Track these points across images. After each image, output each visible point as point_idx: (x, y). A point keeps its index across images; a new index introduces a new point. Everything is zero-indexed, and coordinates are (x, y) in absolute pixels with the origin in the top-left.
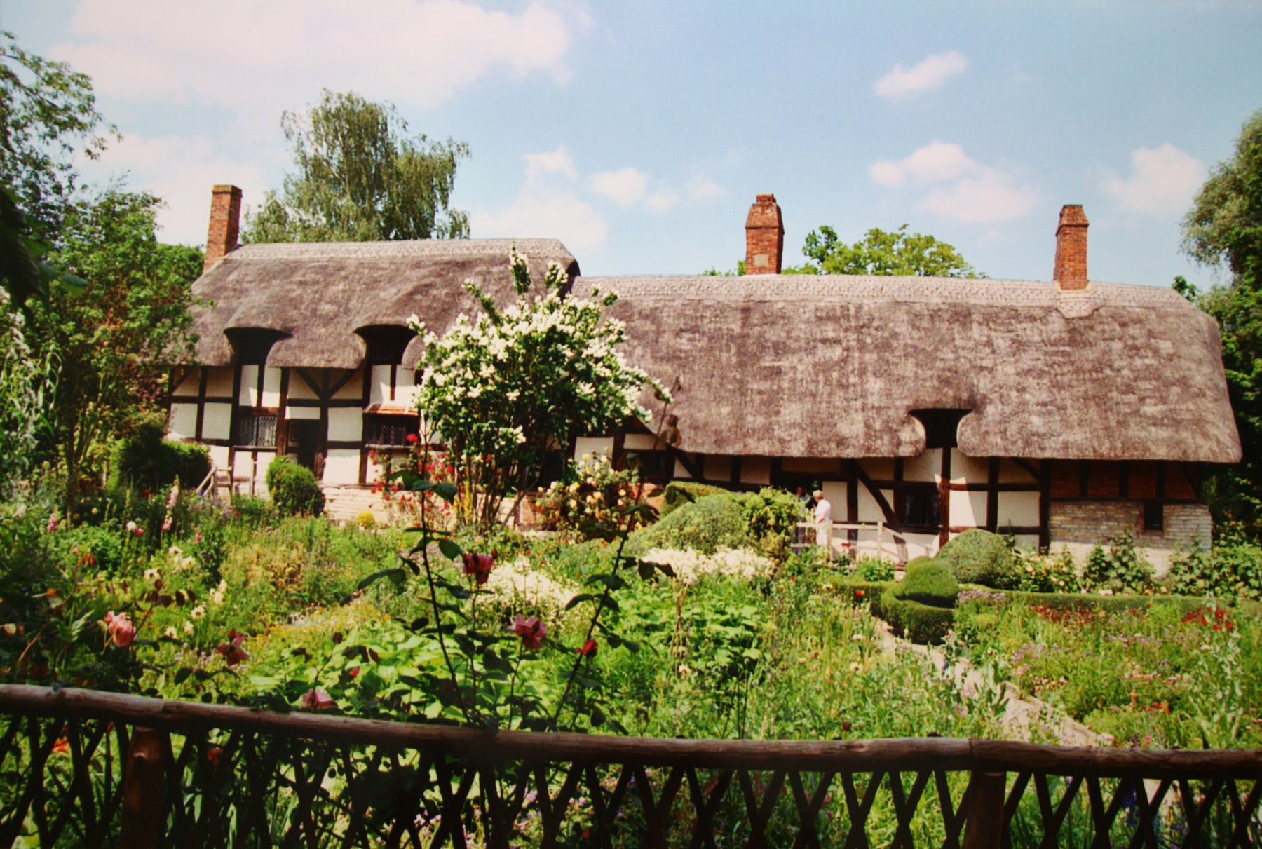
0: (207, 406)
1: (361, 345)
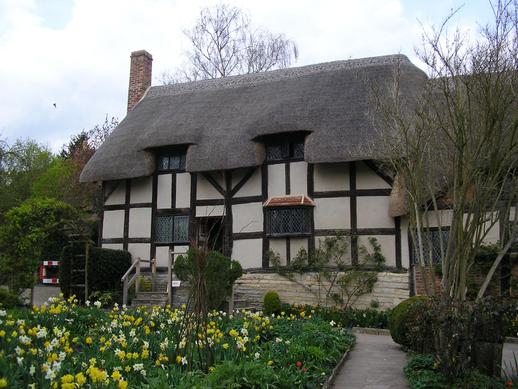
0: (132, 211)
1: (256, 147)
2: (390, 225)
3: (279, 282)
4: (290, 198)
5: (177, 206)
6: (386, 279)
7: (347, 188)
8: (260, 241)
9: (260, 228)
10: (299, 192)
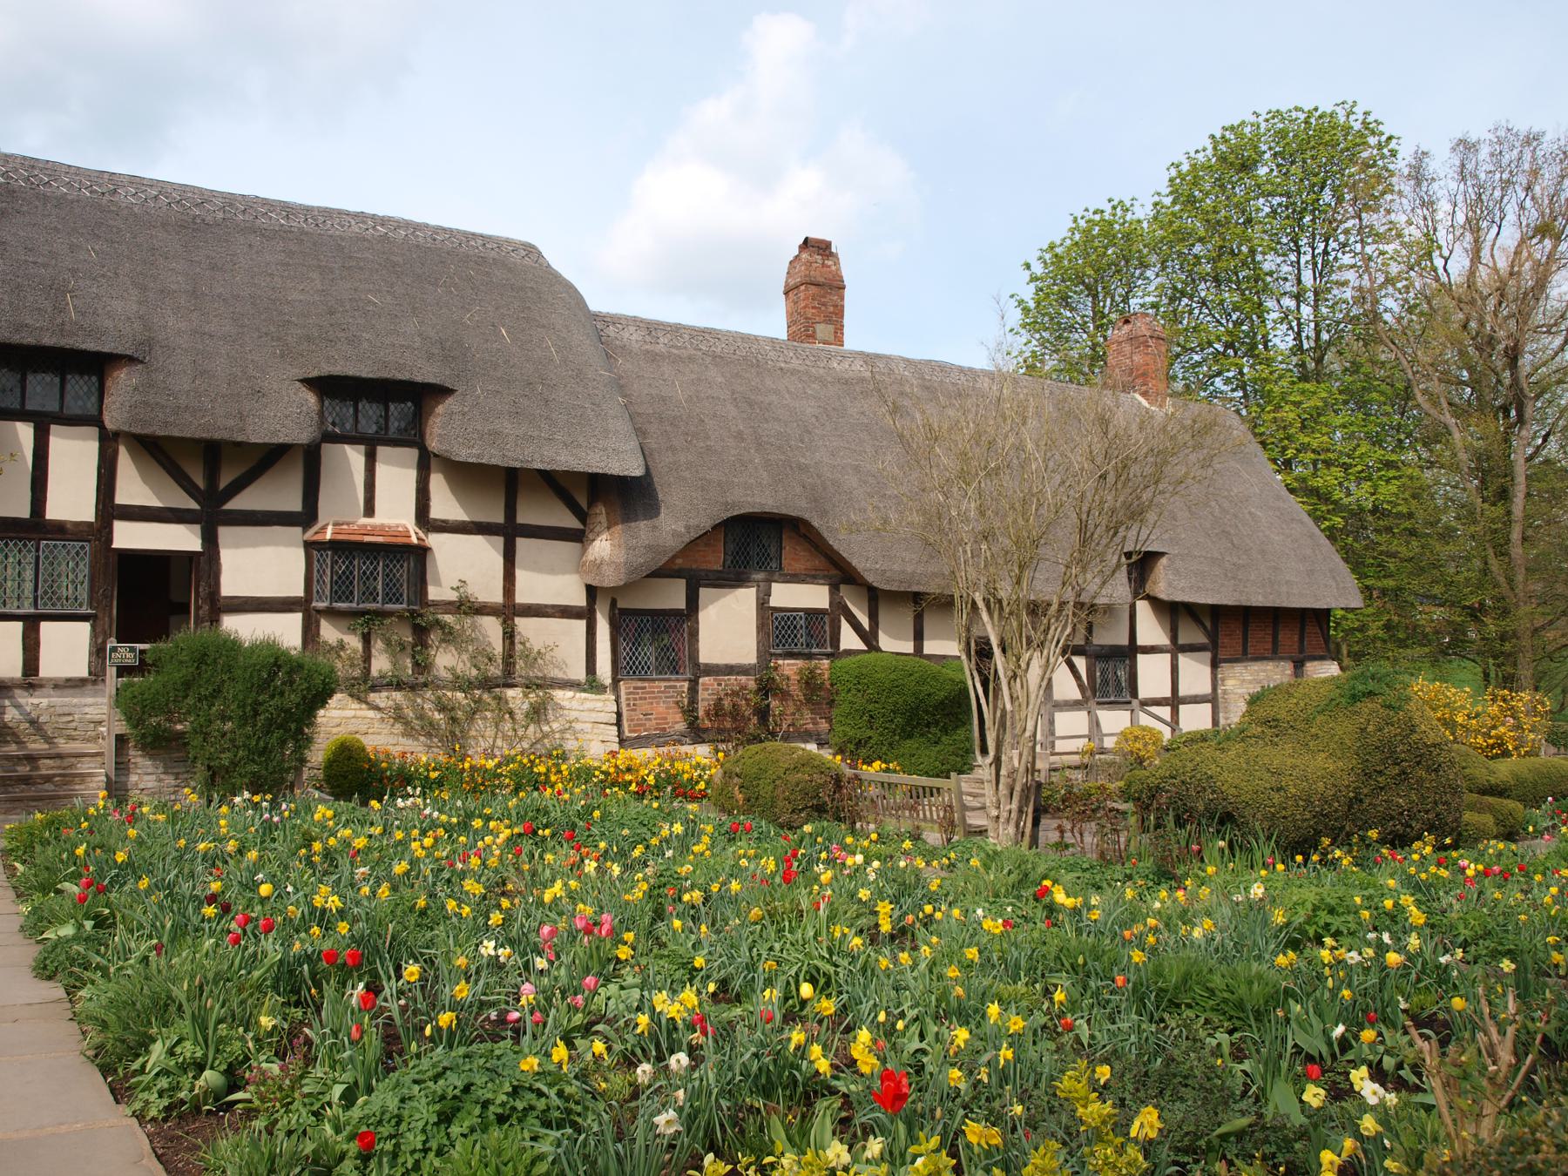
2: (580, 600)
3: (350, 713)
4: (374, 527)
5: (53, 512)
6: (575, 704)
7: (498, 517)
8: (296, 619)
9: (298, 591)
10: (394, 512)
